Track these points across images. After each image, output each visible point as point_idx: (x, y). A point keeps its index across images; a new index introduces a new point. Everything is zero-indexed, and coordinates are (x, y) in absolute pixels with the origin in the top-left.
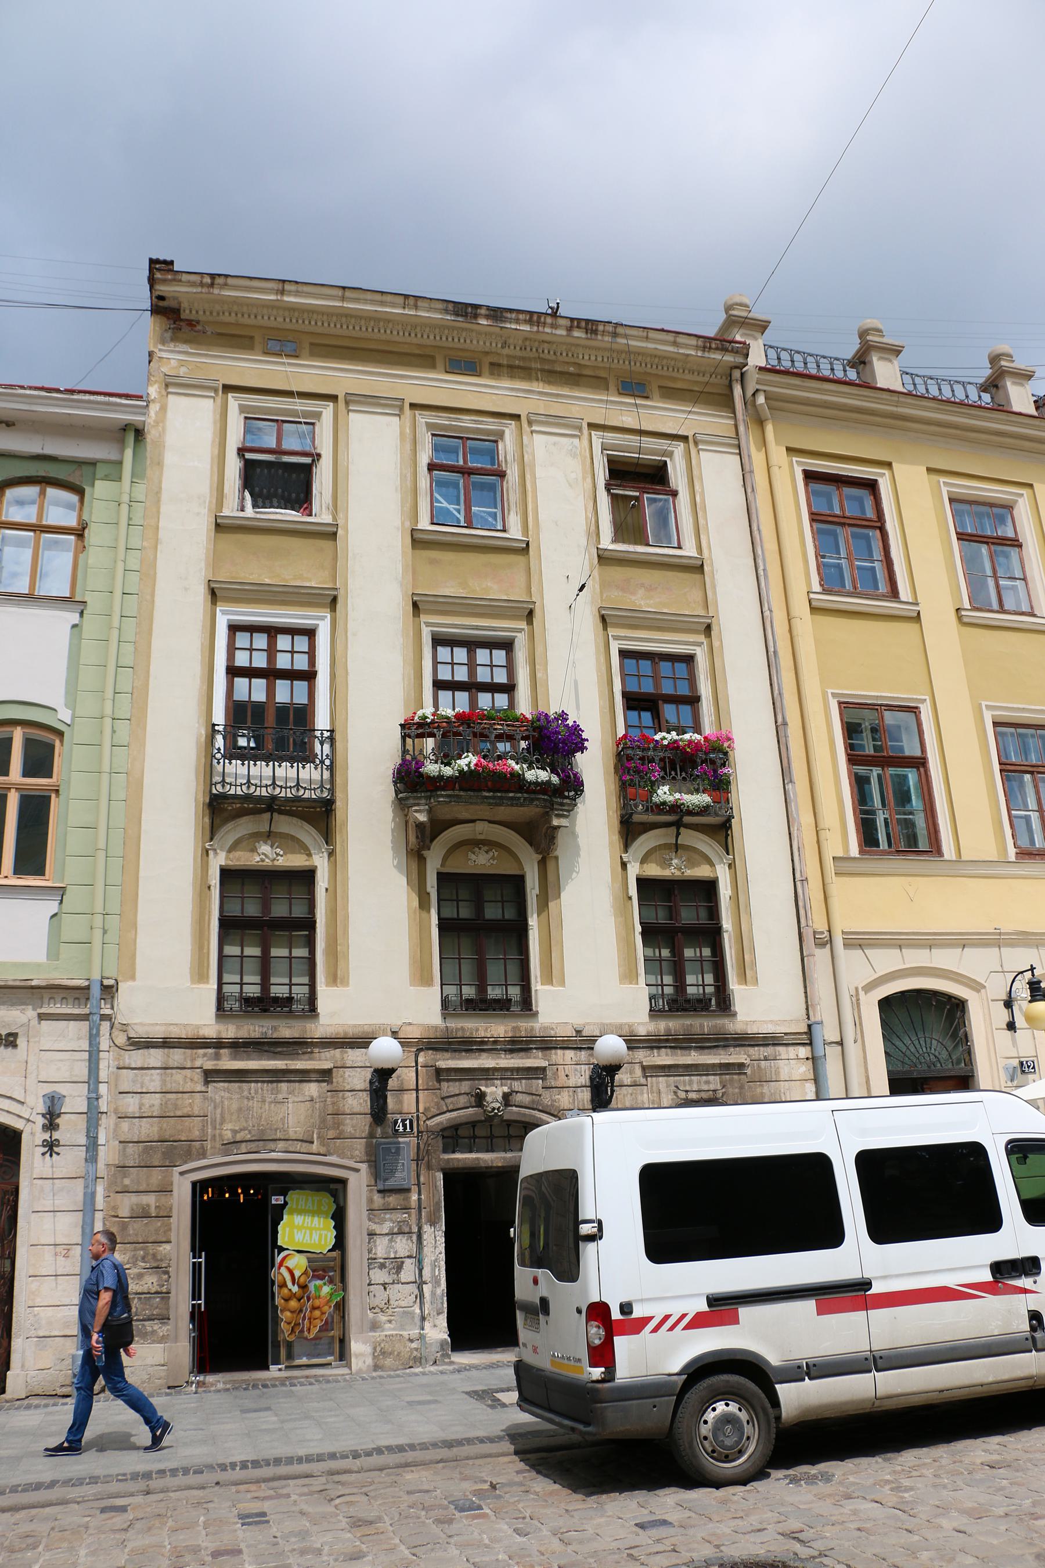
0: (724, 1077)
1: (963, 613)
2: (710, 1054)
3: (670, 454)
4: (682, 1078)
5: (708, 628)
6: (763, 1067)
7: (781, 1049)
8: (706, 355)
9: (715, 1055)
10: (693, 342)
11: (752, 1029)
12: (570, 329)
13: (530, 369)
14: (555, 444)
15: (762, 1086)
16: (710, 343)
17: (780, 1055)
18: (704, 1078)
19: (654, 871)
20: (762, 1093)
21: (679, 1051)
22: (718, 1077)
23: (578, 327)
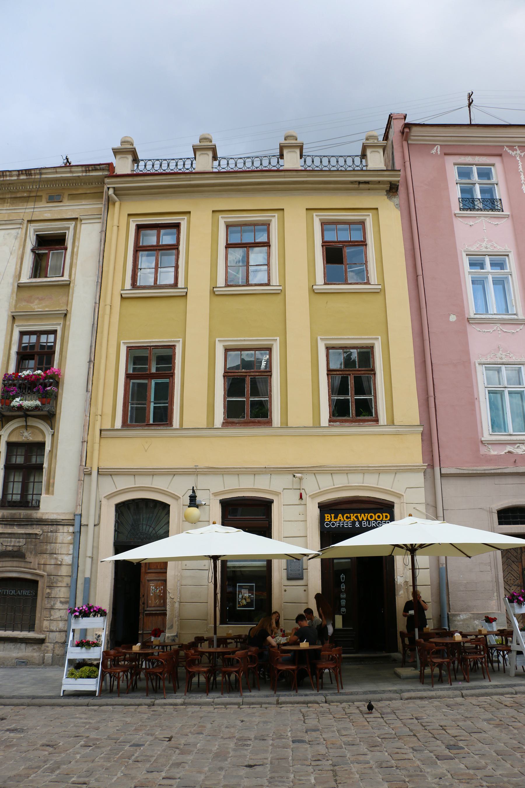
0: (28, 539)
1: (215, 289)
2: (23, 528)
3: (68, 228)
4: (7, 539)
5: (66, 315)
6: (49, 536)
7: (60, 527)
8: (88, 174)
9: (26, 529)
10: (80, 169)
11: (45, 517)
12: (19, 175)
13: (5, 198)
14: (8, 234)
15: (47, 545)
16: (88, 168)
17: (59, 530)
18: (18, 540)
19: (14, 439)
20: (46, 549)
21: (8, 527)
22: (24, 540)
23: (22, 174)
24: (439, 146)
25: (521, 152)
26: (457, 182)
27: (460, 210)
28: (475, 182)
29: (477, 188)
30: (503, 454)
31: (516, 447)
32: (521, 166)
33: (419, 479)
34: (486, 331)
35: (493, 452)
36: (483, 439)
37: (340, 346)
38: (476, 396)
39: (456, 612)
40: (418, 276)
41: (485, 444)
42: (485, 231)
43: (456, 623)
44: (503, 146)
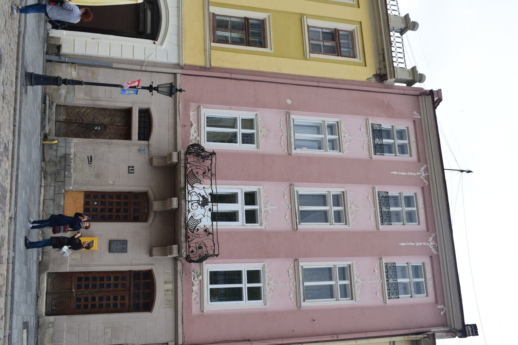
24: (420, 117)
25: (424, 176)
26: (394, 127)
27: (371, 124)
28: (395, 139)
29: (391, 141)
30: (190, 120)
31: (196, 130)
32: (413, 174)
33: (174, 60)
34: (281, 124)
35: (191, 113)
36: (201, 107)
37: (265, 29)
38: (232, 107)
39: (78, 69)
40: (318, 82)
41: (198, 109)
42: (358, 139)
43: (70, 68)
44: (427, 164)
